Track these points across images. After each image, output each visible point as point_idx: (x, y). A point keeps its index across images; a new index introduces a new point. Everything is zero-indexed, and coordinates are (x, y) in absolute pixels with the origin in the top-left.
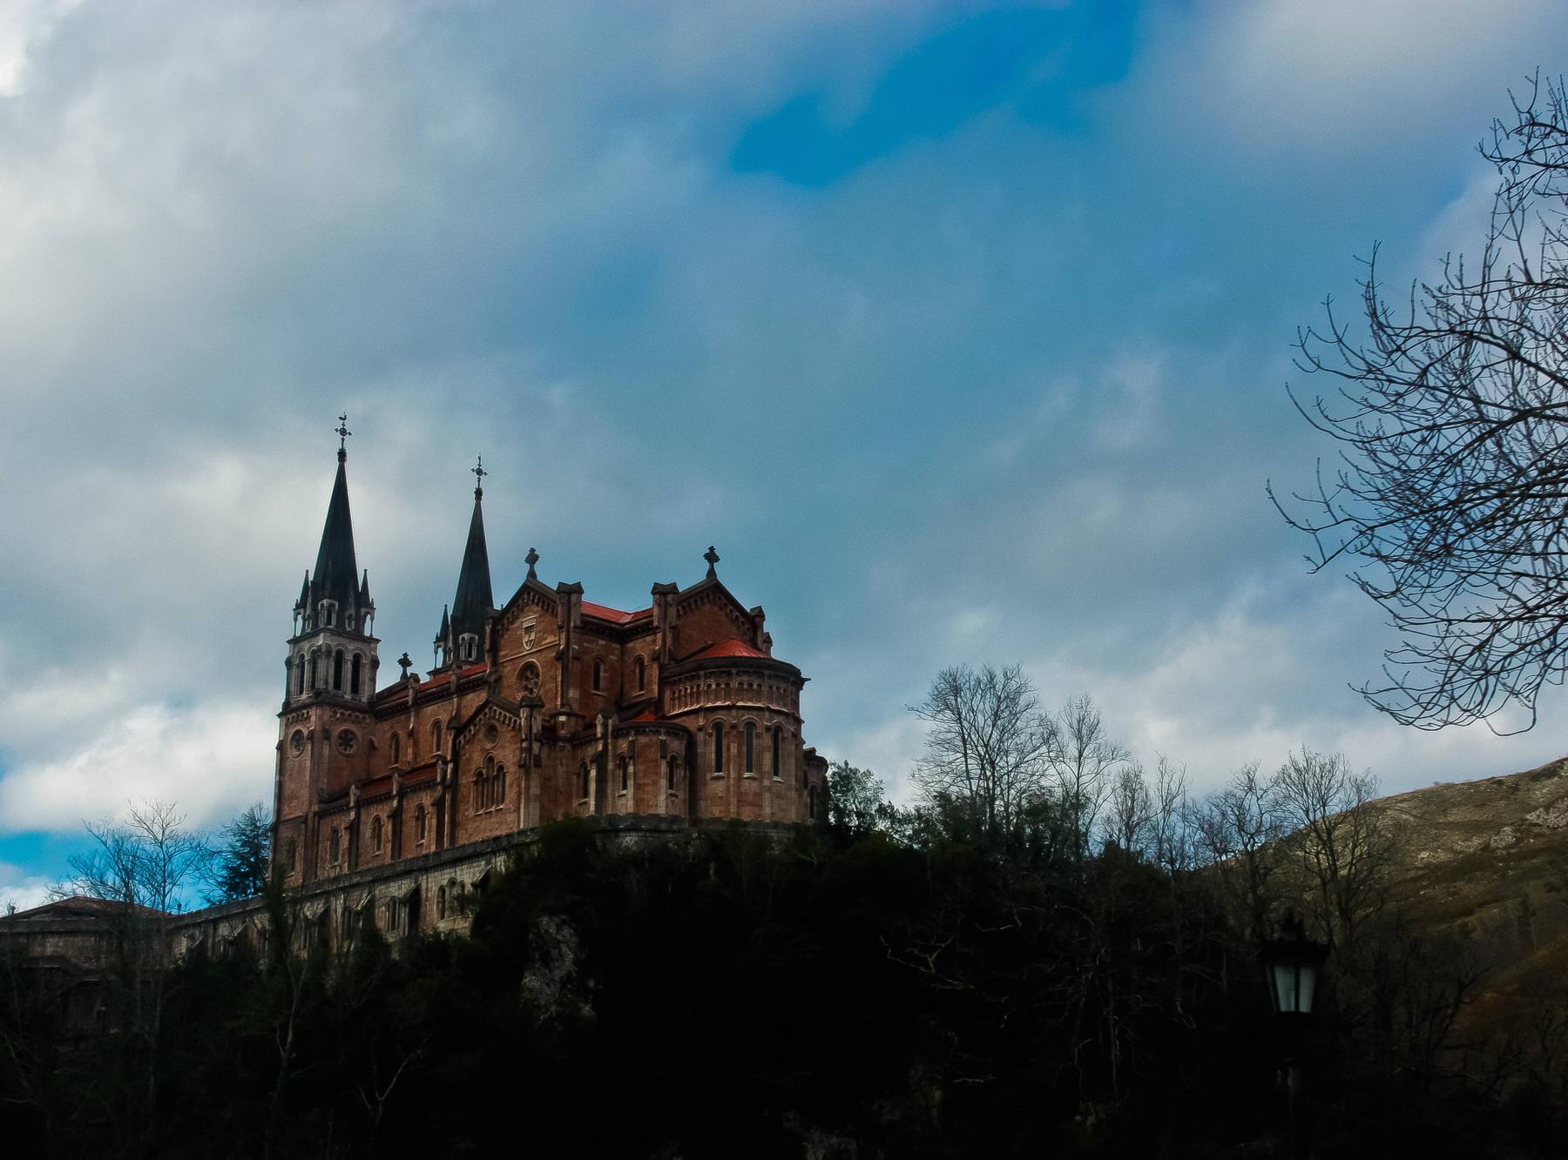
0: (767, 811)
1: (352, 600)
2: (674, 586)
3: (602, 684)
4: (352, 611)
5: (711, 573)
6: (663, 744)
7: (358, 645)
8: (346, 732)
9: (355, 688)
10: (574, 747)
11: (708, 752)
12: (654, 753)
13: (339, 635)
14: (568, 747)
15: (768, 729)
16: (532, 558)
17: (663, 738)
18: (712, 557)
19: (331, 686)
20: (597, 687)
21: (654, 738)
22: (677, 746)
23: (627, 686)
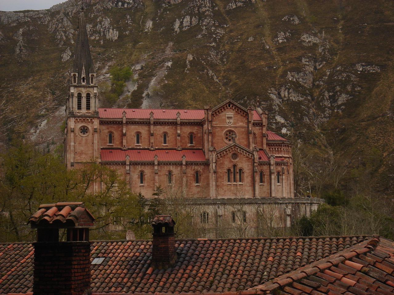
4: (83, 76)
7: (88, 89)
8: (84, 127)
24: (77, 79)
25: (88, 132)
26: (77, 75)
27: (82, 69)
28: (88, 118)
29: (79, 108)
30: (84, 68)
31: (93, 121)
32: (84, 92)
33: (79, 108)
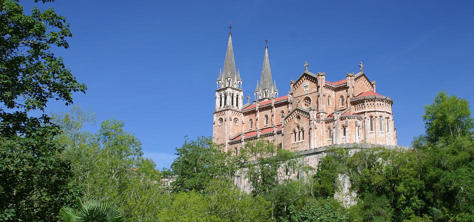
0: (387, 143)
6: (356, 122)
7: (238, 92)
9: (237, 106)
10: (326, 123)
14: (324, 122)
20: (329, 105)
22: (360, 123)
23: (337, 105)
29: (232, 104)
33: (232, 104)
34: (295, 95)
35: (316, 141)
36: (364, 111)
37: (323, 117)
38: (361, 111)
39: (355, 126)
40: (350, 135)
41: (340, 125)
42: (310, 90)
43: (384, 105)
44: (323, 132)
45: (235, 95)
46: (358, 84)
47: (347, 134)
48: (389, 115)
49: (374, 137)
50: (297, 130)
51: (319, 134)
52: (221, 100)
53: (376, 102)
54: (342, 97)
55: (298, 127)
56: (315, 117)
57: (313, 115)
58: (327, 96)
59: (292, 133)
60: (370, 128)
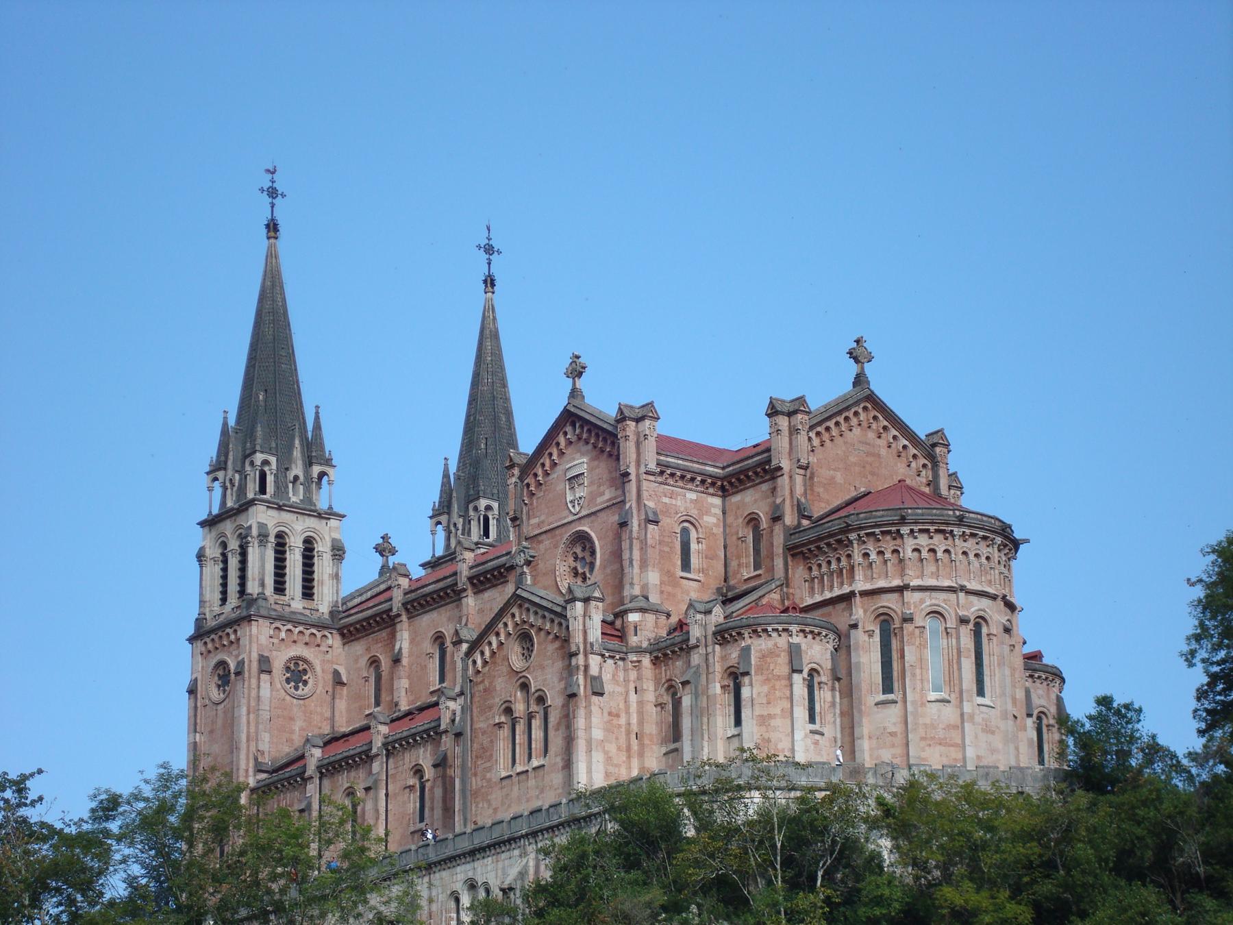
0: (970, 753)
1: (297, 453)
2: (801, 400)
3: (695, 561)
5: (860, 380)
6: (794, 653)
7: (312, 522)
8: (297, 659)
9: (308, 593)
10: (656, 662)
11: (868, 659)
12: (781, 666)
13: (280, 508)
14: (646, 661)
15: (964, 621)
16: (576, 371)
17: (795, 640)
18: (858, 354)
19: (269, 590)
20: (686, 566)
21: (782, 641)
22: (818, 652)
23: (734, 564)
24: (270, 479)
25: (311, 682)
26: (274, 466)
27: (291, 447)
28: (314, 631)
29: (280, 588)
30: (297, 442)
31: (330, 642)
32: (298, 528)
33: (280, 588)
34: (531, 526)
35: (598, 757)
36: (846, 589)
37: (646, 628)
38: (837, 592)
39: (785, 670)
40: (763, 720)
41: (718, 668)
42: (592, 497)
43: (957, 555)
44: (641, 713)
45: (295, 544)
46: (835, 449)
47: (746, 713)
48: (985, 603)
49: (898, 729)
50: (519, 708)
51: (623, 721)
52: (225, 570)
53: (910, 543)
54: (753, 520)
55: (525, 687)
56: (595, 633)
57: (588, 623)
58: (671, 524)
59: (499, 725)
60: (879, 679)
